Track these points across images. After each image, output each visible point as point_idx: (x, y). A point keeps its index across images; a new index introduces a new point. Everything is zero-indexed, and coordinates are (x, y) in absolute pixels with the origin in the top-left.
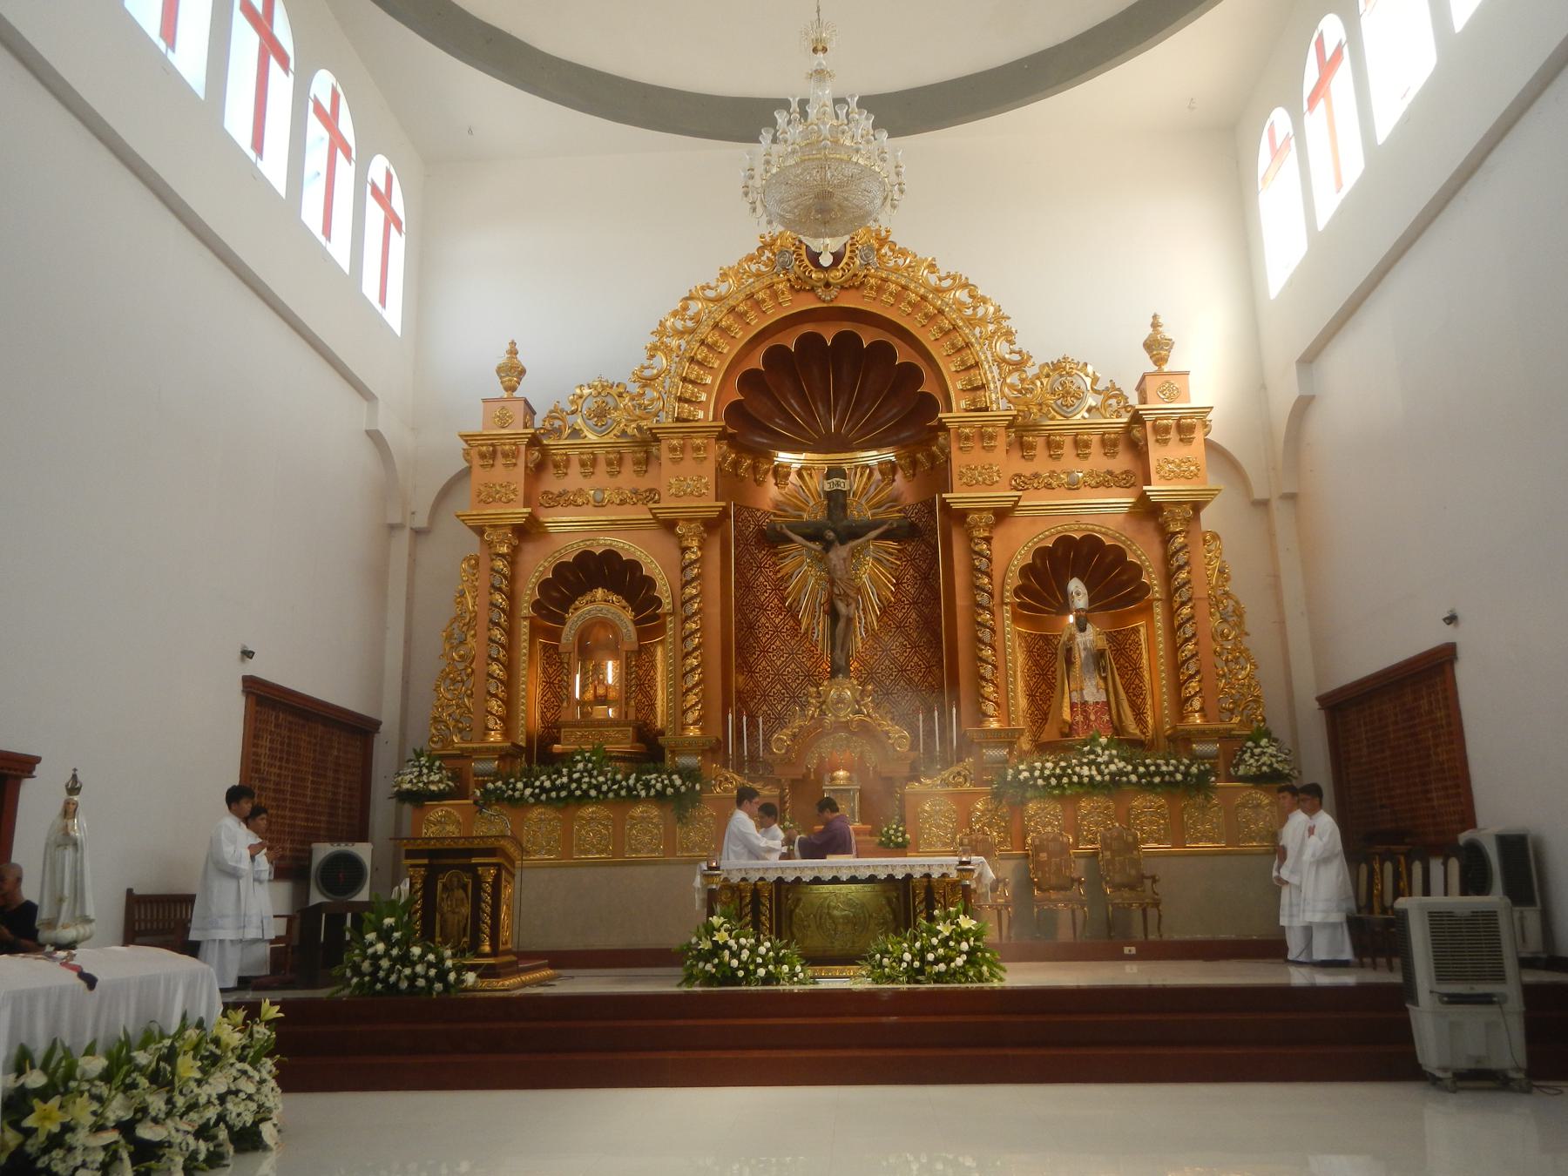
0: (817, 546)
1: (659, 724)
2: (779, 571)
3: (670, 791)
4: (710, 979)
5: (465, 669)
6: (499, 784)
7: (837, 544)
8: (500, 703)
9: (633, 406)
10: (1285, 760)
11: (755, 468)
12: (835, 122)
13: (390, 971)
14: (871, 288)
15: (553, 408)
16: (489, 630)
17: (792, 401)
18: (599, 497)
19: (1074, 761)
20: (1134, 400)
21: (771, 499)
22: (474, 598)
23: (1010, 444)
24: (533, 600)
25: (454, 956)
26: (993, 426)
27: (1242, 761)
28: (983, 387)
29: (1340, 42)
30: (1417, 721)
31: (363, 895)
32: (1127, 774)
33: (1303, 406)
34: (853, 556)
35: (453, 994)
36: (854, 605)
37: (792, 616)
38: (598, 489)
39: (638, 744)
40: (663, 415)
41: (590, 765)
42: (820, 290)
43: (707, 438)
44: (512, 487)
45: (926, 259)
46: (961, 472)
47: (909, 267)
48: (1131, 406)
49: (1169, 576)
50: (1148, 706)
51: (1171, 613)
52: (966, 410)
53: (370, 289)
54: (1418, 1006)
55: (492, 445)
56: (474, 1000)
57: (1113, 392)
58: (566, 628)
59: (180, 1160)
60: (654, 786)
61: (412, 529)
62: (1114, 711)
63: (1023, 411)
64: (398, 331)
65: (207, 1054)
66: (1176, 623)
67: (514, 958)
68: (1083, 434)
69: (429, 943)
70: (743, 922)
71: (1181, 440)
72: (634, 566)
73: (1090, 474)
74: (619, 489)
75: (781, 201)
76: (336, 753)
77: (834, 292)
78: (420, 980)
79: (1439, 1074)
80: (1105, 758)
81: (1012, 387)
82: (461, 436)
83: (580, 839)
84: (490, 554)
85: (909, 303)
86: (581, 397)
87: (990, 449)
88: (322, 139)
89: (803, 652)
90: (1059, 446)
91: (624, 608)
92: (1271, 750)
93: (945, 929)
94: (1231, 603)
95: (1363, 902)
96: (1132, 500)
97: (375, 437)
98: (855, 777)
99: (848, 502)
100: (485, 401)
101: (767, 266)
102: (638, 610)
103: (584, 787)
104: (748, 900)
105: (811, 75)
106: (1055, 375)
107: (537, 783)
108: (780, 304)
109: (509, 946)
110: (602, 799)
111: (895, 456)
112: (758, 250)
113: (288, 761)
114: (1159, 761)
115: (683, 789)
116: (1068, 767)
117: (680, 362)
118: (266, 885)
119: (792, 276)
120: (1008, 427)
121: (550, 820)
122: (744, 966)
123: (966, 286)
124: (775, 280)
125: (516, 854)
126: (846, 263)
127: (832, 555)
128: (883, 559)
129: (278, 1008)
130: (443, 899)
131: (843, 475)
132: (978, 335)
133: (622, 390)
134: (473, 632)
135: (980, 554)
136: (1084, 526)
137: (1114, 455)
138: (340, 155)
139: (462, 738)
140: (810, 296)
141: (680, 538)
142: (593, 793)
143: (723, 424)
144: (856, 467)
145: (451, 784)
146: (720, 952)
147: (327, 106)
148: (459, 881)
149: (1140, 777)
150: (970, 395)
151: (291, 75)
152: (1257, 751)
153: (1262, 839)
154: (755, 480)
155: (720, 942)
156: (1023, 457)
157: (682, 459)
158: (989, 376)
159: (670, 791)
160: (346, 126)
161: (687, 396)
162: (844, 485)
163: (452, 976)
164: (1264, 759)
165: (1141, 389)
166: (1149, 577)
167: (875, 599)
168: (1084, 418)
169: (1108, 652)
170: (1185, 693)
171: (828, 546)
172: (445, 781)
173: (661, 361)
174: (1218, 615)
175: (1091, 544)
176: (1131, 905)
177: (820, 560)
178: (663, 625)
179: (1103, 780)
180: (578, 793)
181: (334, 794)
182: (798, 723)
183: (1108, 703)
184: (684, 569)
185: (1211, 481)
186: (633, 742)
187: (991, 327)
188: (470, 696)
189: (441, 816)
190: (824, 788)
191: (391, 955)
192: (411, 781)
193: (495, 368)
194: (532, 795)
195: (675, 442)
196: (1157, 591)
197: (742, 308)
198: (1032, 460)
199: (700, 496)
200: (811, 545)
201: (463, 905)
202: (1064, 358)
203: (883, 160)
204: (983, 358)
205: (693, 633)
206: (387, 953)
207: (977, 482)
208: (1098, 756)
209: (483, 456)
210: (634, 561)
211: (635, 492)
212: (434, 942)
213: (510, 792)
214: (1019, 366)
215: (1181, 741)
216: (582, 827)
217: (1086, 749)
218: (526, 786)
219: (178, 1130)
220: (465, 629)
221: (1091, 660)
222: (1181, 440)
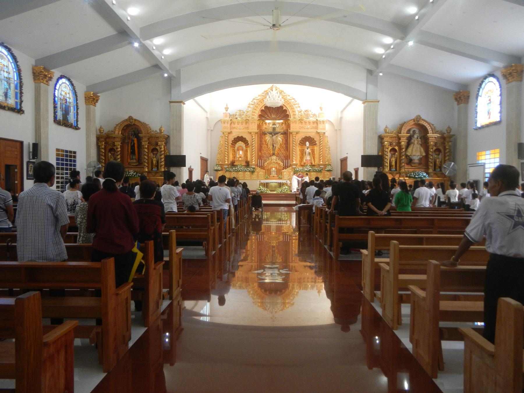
0: (271, 135)
11: (262, 123)
33: (341, 118)
57: (314, 115)
72: (245, 139)
93: (284, 188)
97: (207, 118)
100: (224, 113)
123: (294, 99)
127: (273, 137)
141: (252, 135)
162: (275, 126)
171: (273, 136)
173: (250, 109)
209: (224, 122)
211: (245, 127)
214: (301, 112)
215: (319, 165)
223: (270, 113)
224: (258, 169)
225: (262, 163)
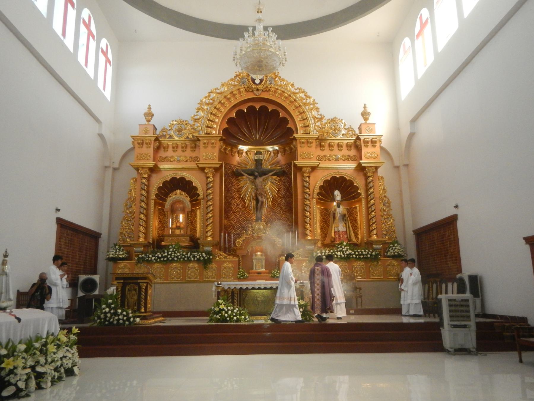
0: (252, 177)
1: (198, 236)
2: (239, 185)
3: (202, 258)
4: (218, 320)
5: (132, 216)
6: (143, 255)
7: (259, 177)
8: (144, 228)
9: (191, 128)
10: (403, 251)
11: (231, 151)
12: (264, 37)
13: (111, 318)
14: (272, 92)
15: (163, 128)
16: (140, 203)
17: (245, 128)
18: (179, 159)
19: (335, 250)
20: (357, 132)
21: (237, 161)
22: (135, 192)
23: (317, 145)
24: (156, 193)
25: (132, 313)
26: (312, 139)
27: (389, 251)
28: (308, 126)
29: (427, 18)
30: (444, 239)
31: (97, 292)
32: (352, 255)
33: (411, 136)
34: (264, 181)
35: (132, 325)
36: (264, 197)
37: (243, 200)
38: (178, 156)
39: (190, 243)
40: (201, 132)
41: (175, 250)
42: (255, 92)
43: (216, 140)
44: (149, 155)
45: (291, 83)
46: (301, 154)
47: (285, 85)
48: (356, 134)
49: (367, 190)
50: (359, 233)
51: (367, 202)
52: (303, 134)
53: (100, 85)
54: (444, 328)
55: (142, 140)
56: (139, 327)
57: (350, 129)
58: (167, 203)
59: (50, 378)
60: (196, 257)
61: (113, 168)
62: (348, 234)
63: (321, 135)
64: (109, 100)
65: (56, 344)
66: (369, 206)
67: (151, 314)
68: (340, 143)
69: (123, 308)
70: (229, 302)
71: (372, 146)
72: (190, 183)
73: (343, 156)
74: (185, 157)
75: (246, 63)
76: (86, 244)
77: (260, 92)
78: (121, 321)
79: (450, 350)
80: (345, 249)
81: (318, 126)
82: (131, 137)
83: (171, 274)
84: (141, 177)
85: (285, 97)
86: (173, 124)
87: (310, 147)
88: (85, 32)
89: (246, 212)
90: (333, 146)
91: (187, 197)
92: (398, 248)
94: (387, 199)
95: (426, 296)
96: (356, 165)
97: (101, 136)
98: (263, 254)
99: (263, 163)
100: (140, 125)
101: (237, 82)
102: (191, 197)
103: (173, 257)
104: (230, 294)
105: (256, 20)
106: (332, 123)
107: (156, 255)
108: (242, 95)
109: (150, 310)
110: (179, 260)
111: (279, 148)
112: (234, 77)
113: (71, 247)
114: (362, 251)
115: (206, 258)
116: (333, 252)
117: (207, 114)
118: (65, 289)
119: (246, 87)
120: (316, 140)
121: (161, 268)
122: (229, 316)
123: (303, 92)
124: (240, 87)
125: (153, 279)
126: (264, 83)
127: (257, 180)
128: (274, 183)
129: (78, 329)
130: (128, 294)
131: (260, 153)
132: (307, 109)
133: (187, 123)
134: (134, 204)
135: (306, 181)
136: (340, 173)
137: (350, 150)
138: (91, 38)
139: (130, 240)
140: (252, 93)
141: (206, 173)
142: (176, 259)
143: (222, 135)
144: (265, 151)
145: (127, 255)
146: (221, 311)
147: (87, 21)
148: (133, 288)
149: (356, 255)
150: (304, 129)
151: (75, 9)
152: (394, 248)
153: (395, 276)
154: (232, 155)
155: (222, 308)
156: (321, 150)
157: (207, 147)
158: (311, 123)
159: (202, 258)
160: (93, 28)
161: (210, 125)
162: (261, 157)
163: (132, 319)
164: (396, 250)
165: (360, 128)
166: (361, 191)
167: (271, 196)
168: (341, 137)
169: (347, 215)
170: (371, 229)
171: (256, 177)
172: (125, 254)
173: (201, 114)
174: (382, 203)
175: (342, 179)
176: (352, 297)
177: (253, 182)
178: (200, 202)
179: (344, 257)
180: (170, 259)
181: (86, 258)
182: (245, 237)
183: (346, 231)
184: (207, 184)
185: (381, 159)
186: (189, 241)
187: (312, 106)
188: (133, 226)
189: (123, 266)
190: (253, 258)
191: (111, 312)
192: (113, 254)
193: (143, 113)
194: (155, 259)
195: (205, 141)
196: (363, 195)
197: (229, 96)
198: (324, 151)
199: (213, 159)
200: (250, 177)
201: (135, 296)
202: (335, 117)
203: (280, 50)
204: (309, 116)
205: (210, 206)
206: (109, 312)
207: (306, 158)
208: (343, 248)
209: (139, 144)
210: (190, 181)
211: (191, 158)
212: (125, 308)
213: (147, 258)
214: (320, 119)
215: (369, 244)
216: (171, 270)
217: (339, 246)
218: (152, 256)
219: (49, 369)
220: (131, 203)
221: (341, 217)
222: (372, 146)
223: (248, 128)
224: (220, 256)
225: (229, 241)
